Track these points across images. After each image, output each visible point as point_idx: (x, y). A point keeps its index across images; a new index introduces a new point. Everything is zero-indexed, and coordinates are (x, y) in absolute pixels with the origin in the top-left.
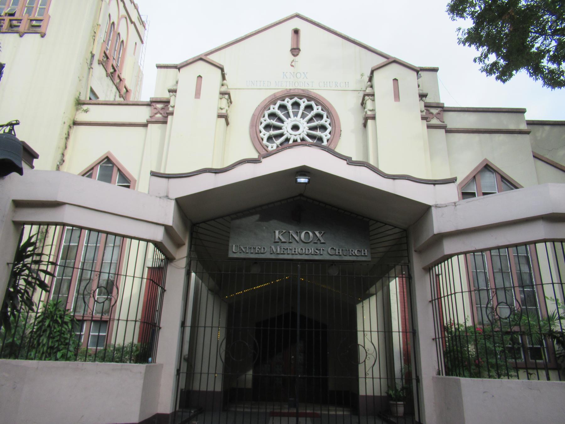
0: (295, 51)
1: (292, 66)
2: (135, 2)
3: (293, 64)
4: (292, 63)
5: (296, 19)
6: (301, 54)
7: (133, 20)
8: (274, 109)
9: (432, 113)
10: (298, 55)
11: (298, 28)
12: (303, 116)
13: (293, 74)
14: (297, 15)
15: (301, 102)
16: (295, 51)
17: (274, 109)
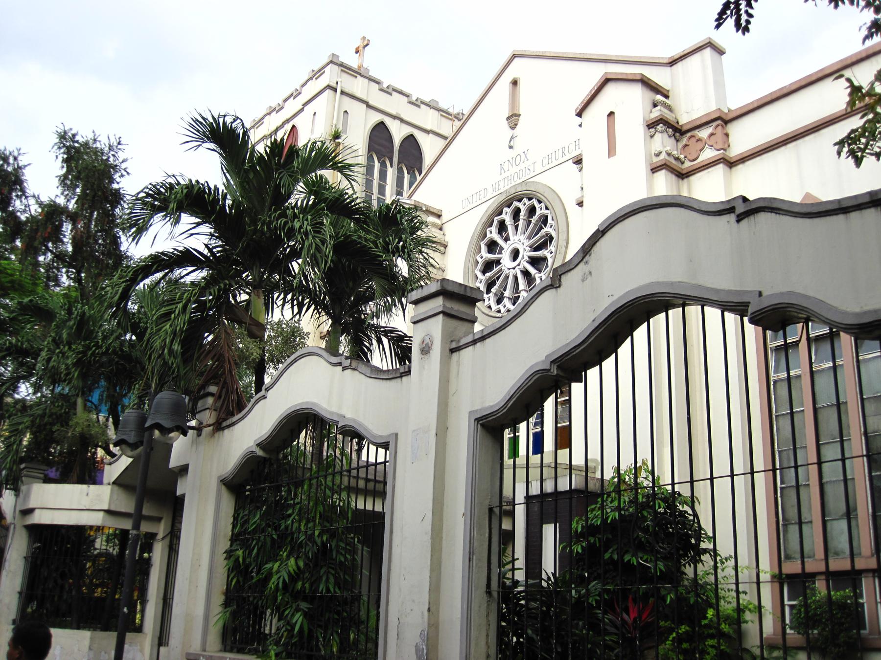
0: (513, 119)
1: (511, 147)
2: (427, 99)
3: (512, 144)
4: (510, 141)
5: (516, 60)
6: (522, 121)
7: (429, 128)
8: (491, 232)
9: (699, 140)
10: (516, 125)
11: (516, 76)
12: (507, 239)
13: (511, 160)
14: (514, 55)
15: (520, 205)
16: (513, 119)
17: (491, 232)
